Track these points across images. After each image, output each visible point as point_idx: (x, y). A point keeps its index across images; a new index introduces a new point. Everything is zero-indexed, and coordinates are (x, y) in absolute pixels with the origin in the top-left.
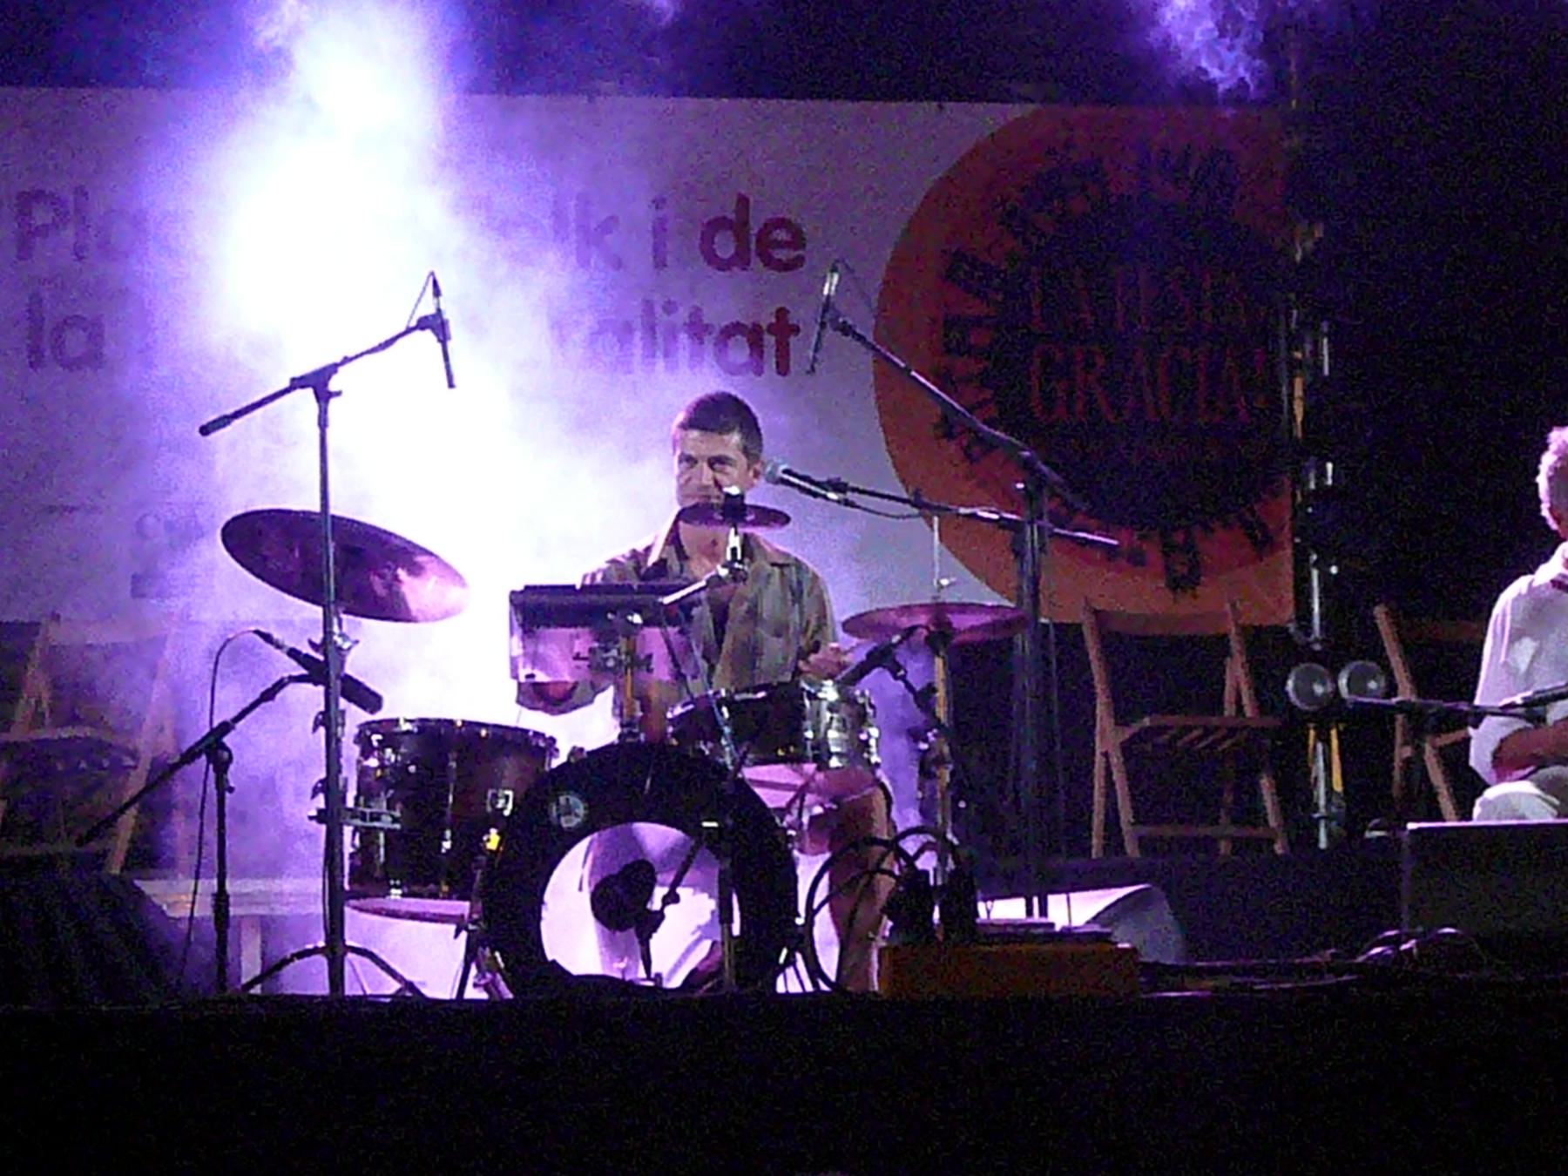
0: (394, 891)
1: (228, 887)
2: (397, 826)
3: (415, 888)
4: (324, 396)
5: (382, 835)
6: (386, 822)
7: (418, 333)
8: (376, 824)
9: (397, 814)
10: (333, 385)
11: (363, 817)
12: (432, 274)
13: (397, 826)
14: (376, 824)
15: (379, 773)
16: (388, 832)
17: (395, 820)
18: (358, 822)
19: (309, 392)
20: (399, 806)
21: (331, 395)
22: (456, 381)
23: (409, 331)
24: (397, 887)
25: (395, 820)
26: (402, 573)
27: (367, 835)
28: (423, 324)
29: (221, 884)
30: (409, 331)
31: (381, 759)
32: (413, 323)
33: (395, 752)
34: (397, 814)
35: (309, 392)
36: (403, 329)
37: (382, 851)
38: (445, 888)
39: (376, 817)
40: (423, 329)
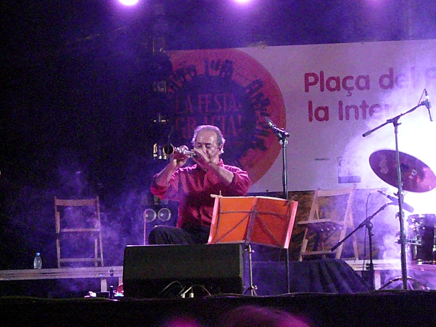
2: (420, 244)
3: (426, 262)
5: (416, 247)
6: (417, 243)
7: (422, 106)
8: (414, 244)
9: (420, 241)
10: (399, 122)
11: (410, 241)
12: (425, 89)
13: (420, 244)
14: (414, 244)
16: (418, 246)
17: (419, 243)
18: (409, 243)
19: (392, 124)
20: (420, 238)
21: (398, 124)
22: (432, 119)
23: (419, 106)
24: (420, 261)
25: (419, 243)
27: (412, 247)
28: (423, 104)
29: (371, 262)
32: (420, 103)
33: (419, 223)
34: (420, 241)
35: (392, 124)
36: (417, 105)
37: (416, 251)
40: (423, 105)
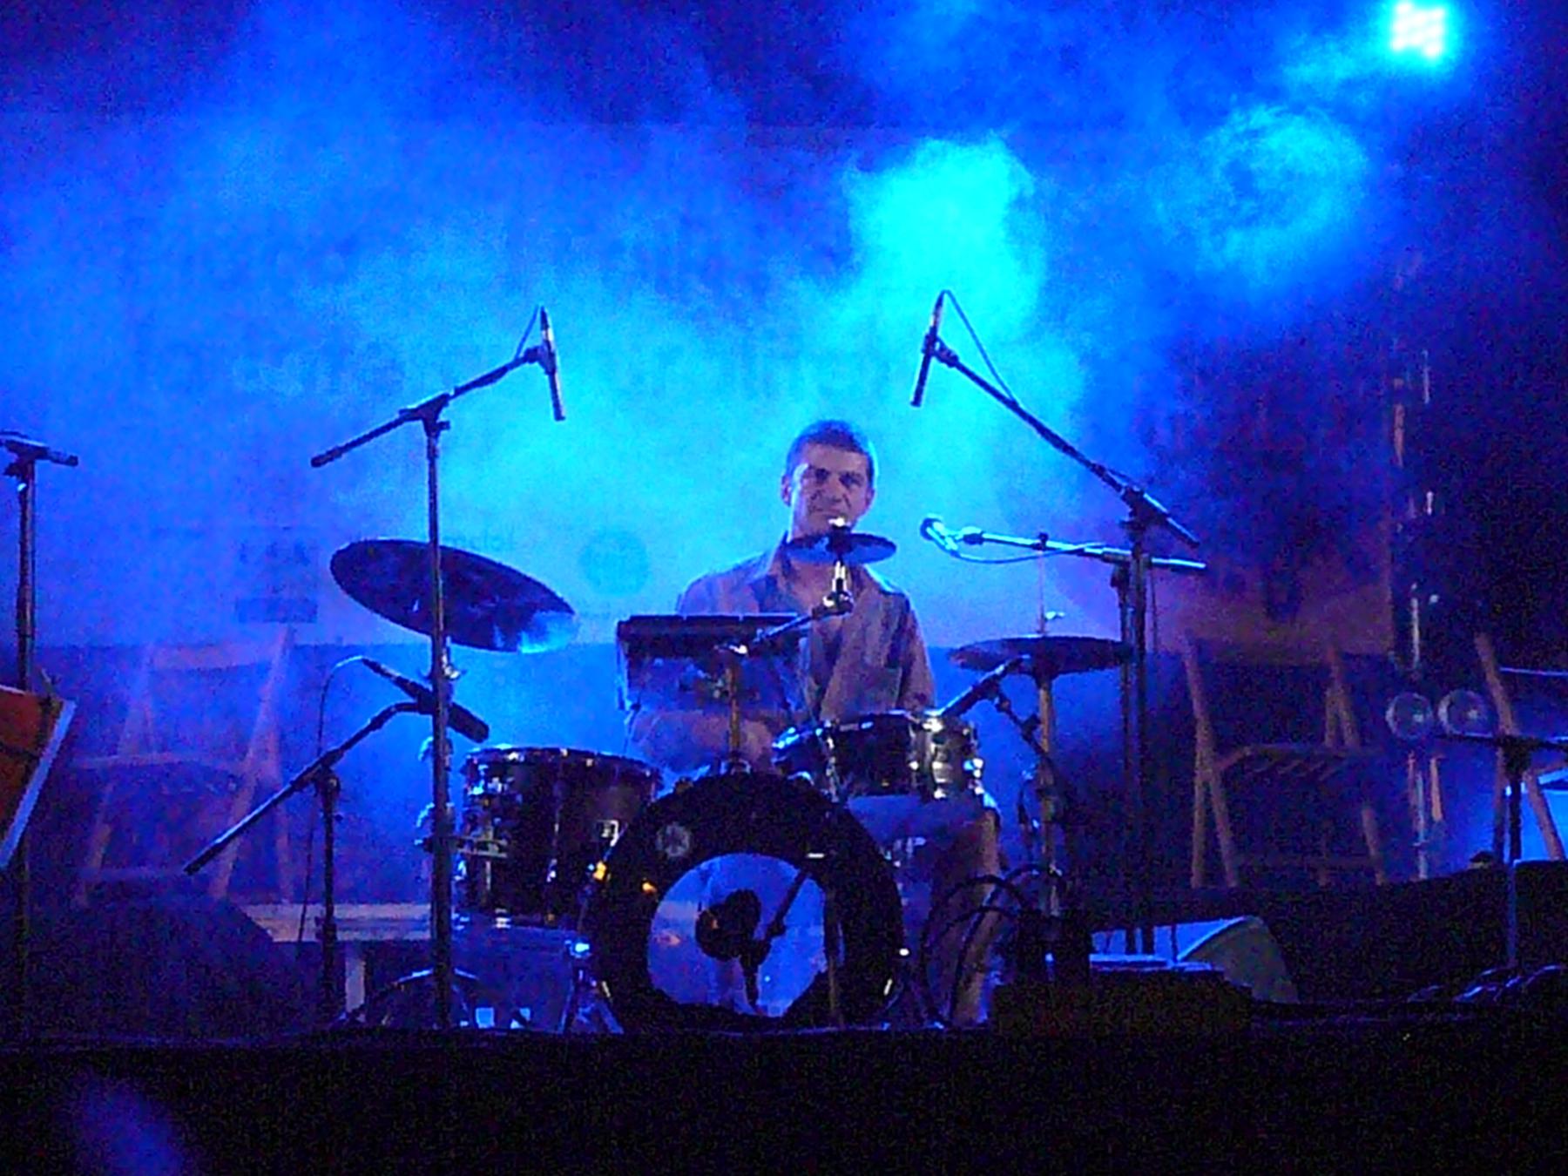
0: (500, 920)
1: (336, 913)
2: (503, 855)
3: (521, 917)
5: (488, 865)
6: (493, 851)
7: (527, 365)
9: (503, 842)
10: (442, 418)
11: (472, 845)
13: (503, 855)
16: (494, 860)
17: (501, 849)
19: (420, 423)
22: (564, 413)
23: (517, 363)
24: (502, 915)
27: (475, 864)
28: (531, 356)
29: (330, 911)
30: (517, 363)
33: (502, 781)
35: (420, 423)
36: (509, 359)
38: (551, 917)
39: (483, 846)
40: (532, 361)
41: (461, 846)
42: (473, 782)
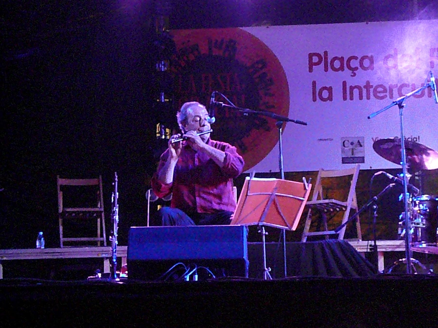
2: (424, 226)
3: (430, 244)
4: (401, 107)
5: (420, 229)
6: (421, 225)
8: (418, 226)
9: (424, 223)
11: (415, 223)
13: (424, 226)
14: (418, 226)
15: (419, 212)
17: (424, 225)
18: (413, 225)
20: (424, 220)
25: (424, 225)
26: (424, 156)
27: (416, 229)
29: (375, 243)
31: (419, 207)
33: (423, 205)
34: (424, 223)
35: (397, 106)
37: (420, 233)
39: (418, 224)
41: (412, 224)
42: (415, 205)
